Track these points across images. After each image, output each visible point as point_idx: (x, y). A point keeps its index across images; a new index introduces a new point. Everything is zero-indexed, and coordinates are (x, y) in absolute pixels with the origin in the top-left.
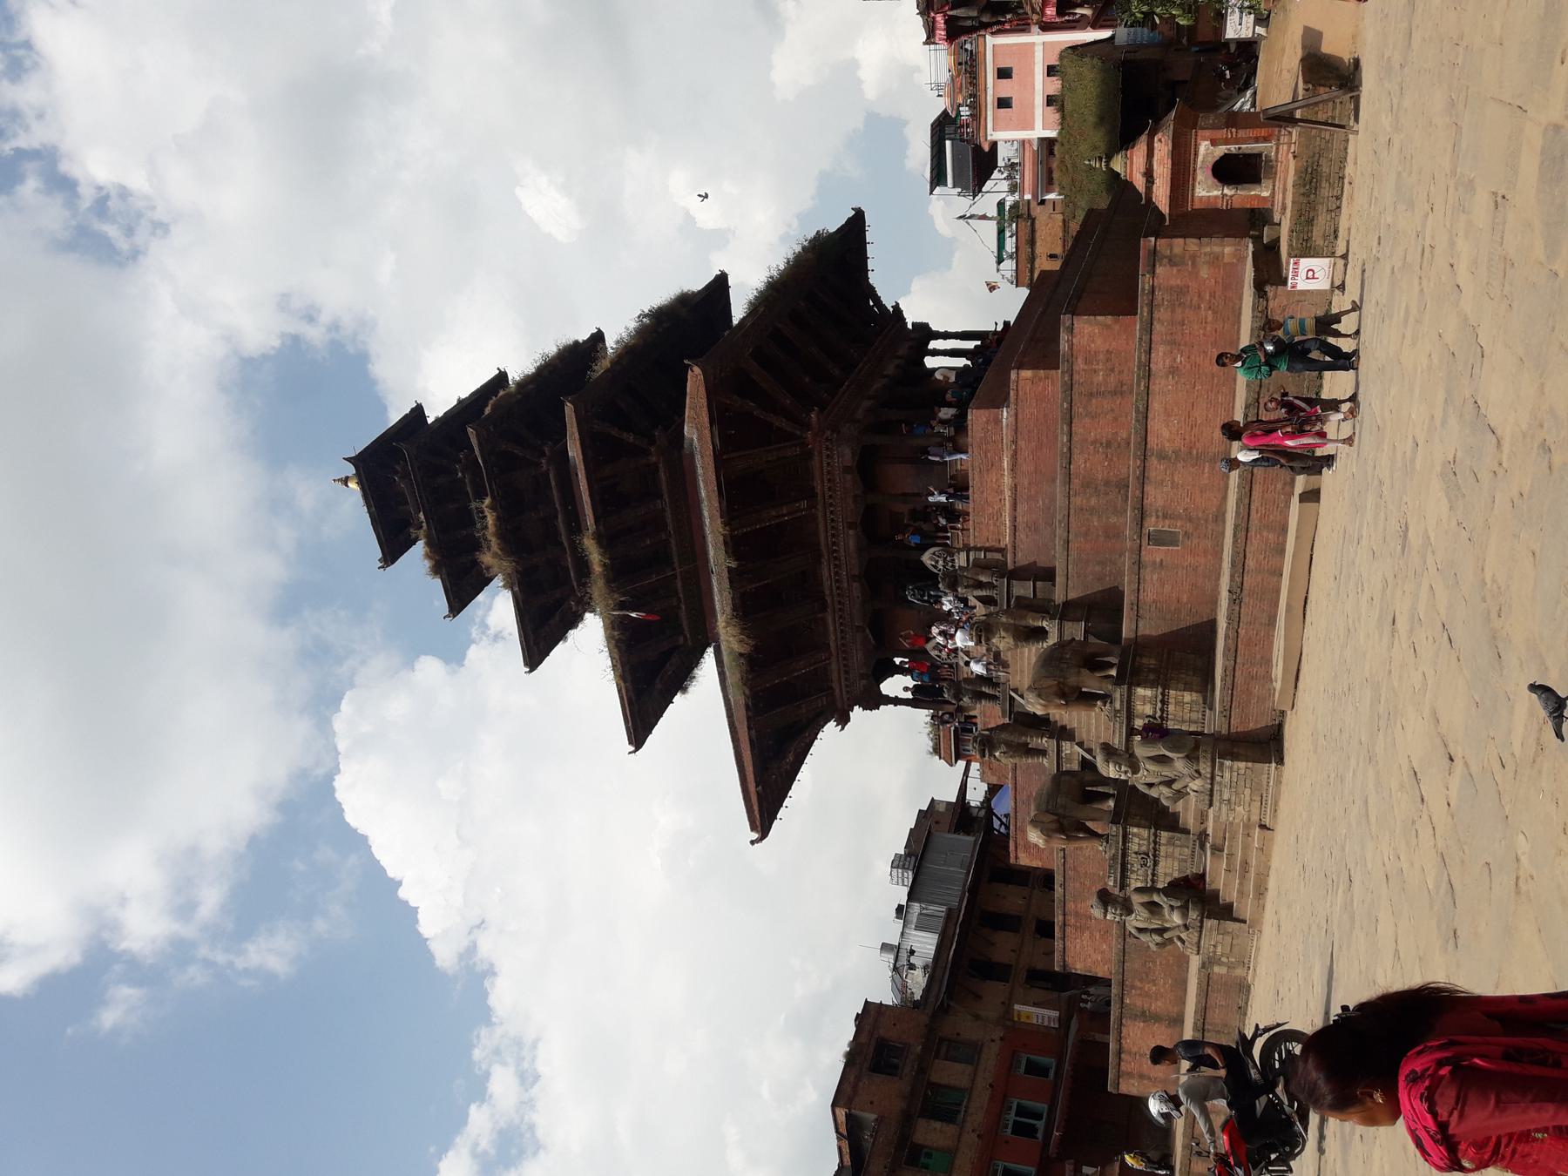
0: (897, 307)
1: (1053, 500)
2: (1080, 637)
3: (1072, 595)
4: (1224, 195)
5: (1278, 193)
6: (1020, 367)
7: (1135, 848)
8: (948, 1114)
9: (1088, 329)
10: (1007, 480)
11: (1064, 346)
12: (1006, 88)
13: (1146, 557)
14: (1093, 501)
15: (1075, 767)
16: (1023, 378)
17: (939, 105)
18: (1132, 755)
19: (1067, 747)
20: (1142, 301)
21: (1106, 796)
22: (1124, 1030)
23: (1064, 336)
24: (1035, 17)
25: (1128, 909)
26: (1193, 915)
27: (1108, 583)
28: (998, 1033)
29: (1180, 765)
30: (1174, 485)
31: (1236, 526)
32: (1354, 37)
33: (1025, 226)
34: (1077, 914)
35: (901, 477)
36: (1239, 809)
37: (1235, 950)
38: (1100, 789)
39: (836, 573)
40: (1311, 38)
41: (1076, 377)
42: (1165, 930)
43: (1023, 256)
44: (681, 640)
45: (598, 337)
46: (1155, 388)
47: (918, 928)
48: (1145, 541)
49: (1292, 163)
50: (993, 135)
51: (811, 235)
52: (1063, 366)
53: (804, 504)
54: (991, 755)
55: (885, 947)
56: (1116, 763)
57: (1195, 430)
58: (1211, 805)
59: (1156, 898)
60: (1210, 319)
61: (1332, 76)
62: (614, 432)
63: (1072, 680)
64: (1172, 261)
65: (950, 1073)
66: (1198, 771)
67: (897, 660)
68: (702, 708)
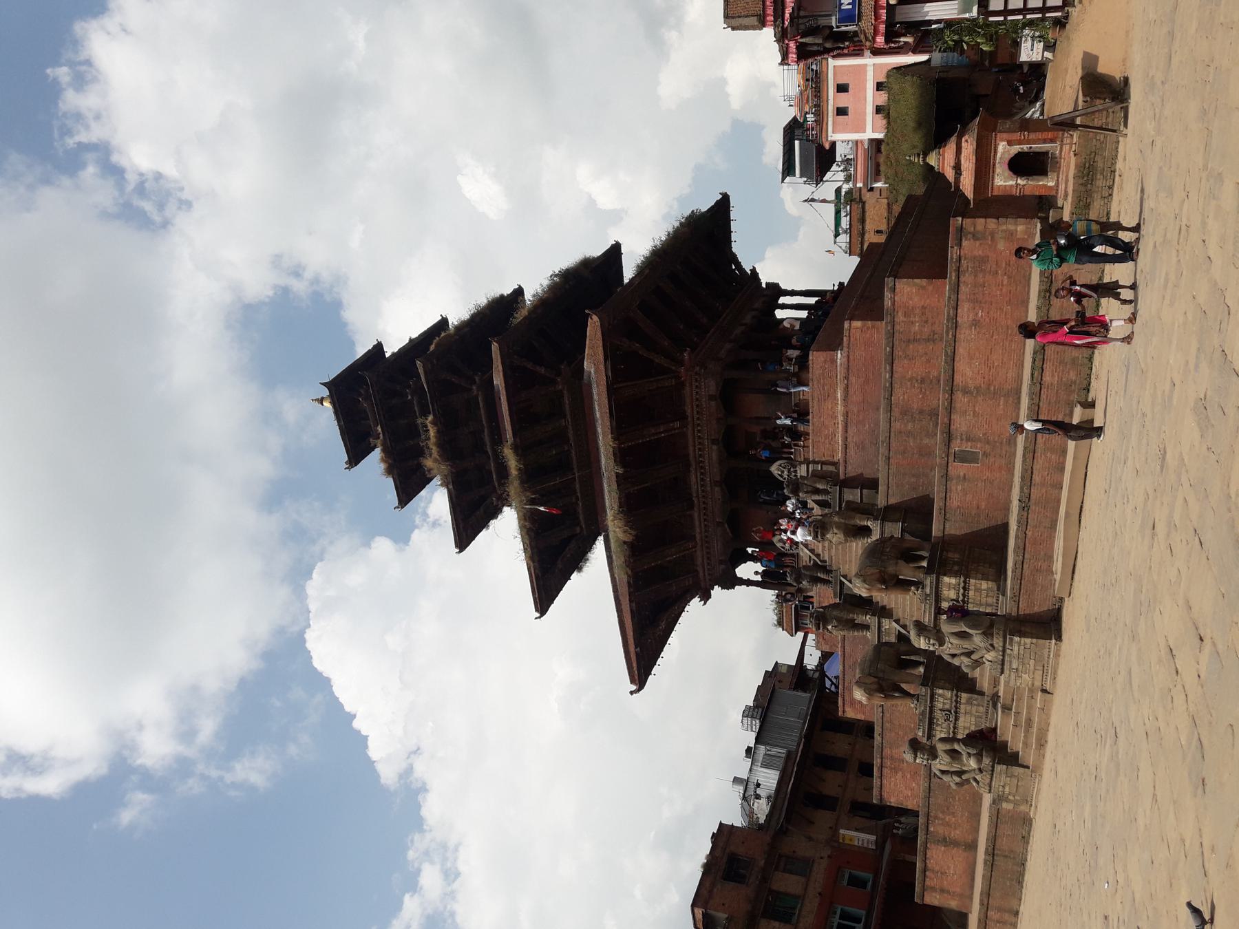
0: (754, 271)
1: (877, 424)
2: (898, 534)
3: (892, 501)
4: (1017, 185)
5: (1062, 183)
6: (851, 319)
7: (940, 706)
9: (907, 289)
10: (840, 408)
11: (887, 303)
12: (843, 100)
14: (910, 426)
15: (893, 639)
16: (854, 327)
17: (791, 113)
18: (939, 631)
19: (886, 623)
20: (951, 267)
21: (918, 664)
22: (929, 854)
23: (887, 294)
24: (868, 44)
25: (933, 754)
26: (987, 761)
28: (826, 852)
29: (978, 640)
31: (1025, 448)
32: (1124, 60)
33: (857, 207)
35: (756, 405)
36: (1025, 676)
37: (1021, 790)
38: (912, 658)
39: (702, 480)
40: (1090, 61)
41: (897, 327)
42: (964, 772)
43: (855, 232)
44: (578, 529)
45: (519, 292)
46: (960, 336)
47: (764, 765)
48: (951, 458)
49: (1073, 160)
50: (832, 136)
51: (688, 213)
52: (887, 319)
53: (677, 424)
54: (825, 628)
55: (737, 780)
56: (926, 637)
57: (993, 370)
58: (1002, 672)
59: (956, 747)
60: (1005, 282)
61: (1106, 90)
62: (530, 365)
63: (891, 569)
64: (975, 237)
65: (787, 883)
66: (992, 645)
67: (750, 550)
68: (593, 584)
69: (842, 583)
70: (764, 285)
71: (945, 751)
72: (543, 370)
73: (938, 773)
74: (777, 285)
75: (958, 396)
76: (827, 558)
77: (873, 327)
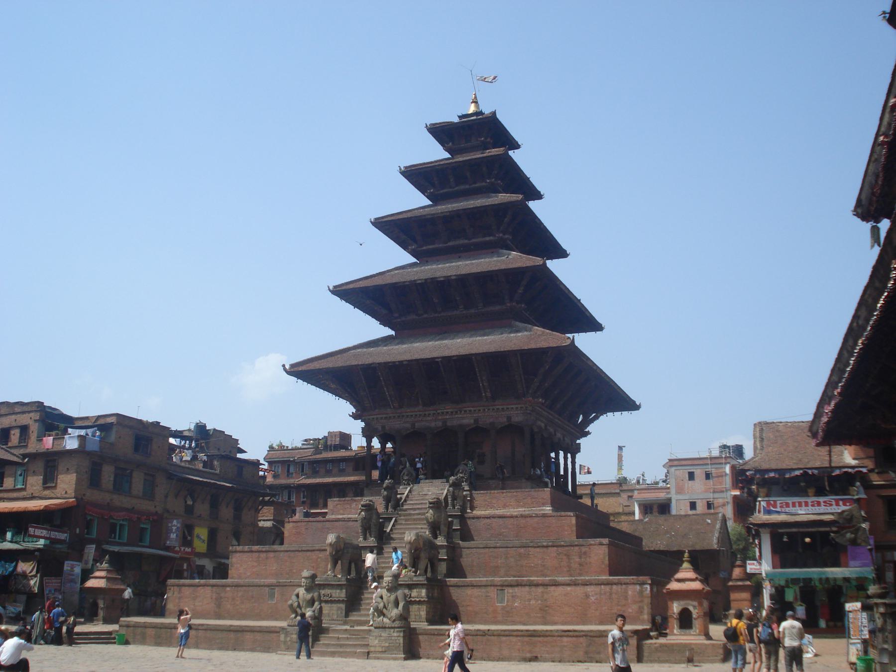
0: (588, 433)
5: (676, 636)
6: (577, 517)
8: (118, 487)
11: (591, 541)
13: (489, 589)
27: (467, 570)
28: (159, 510)
29: (395, 612)
30: (529, 600)
36: (377, 642)
53: (489, 394)
54: (362, 510)
59: (316, 603)
65: (138, 482)
66: (394, 621)
70: (578, 441)
72: (520, 291)
73: (296, 592)
75: (540, 589)
76: (405, 507)
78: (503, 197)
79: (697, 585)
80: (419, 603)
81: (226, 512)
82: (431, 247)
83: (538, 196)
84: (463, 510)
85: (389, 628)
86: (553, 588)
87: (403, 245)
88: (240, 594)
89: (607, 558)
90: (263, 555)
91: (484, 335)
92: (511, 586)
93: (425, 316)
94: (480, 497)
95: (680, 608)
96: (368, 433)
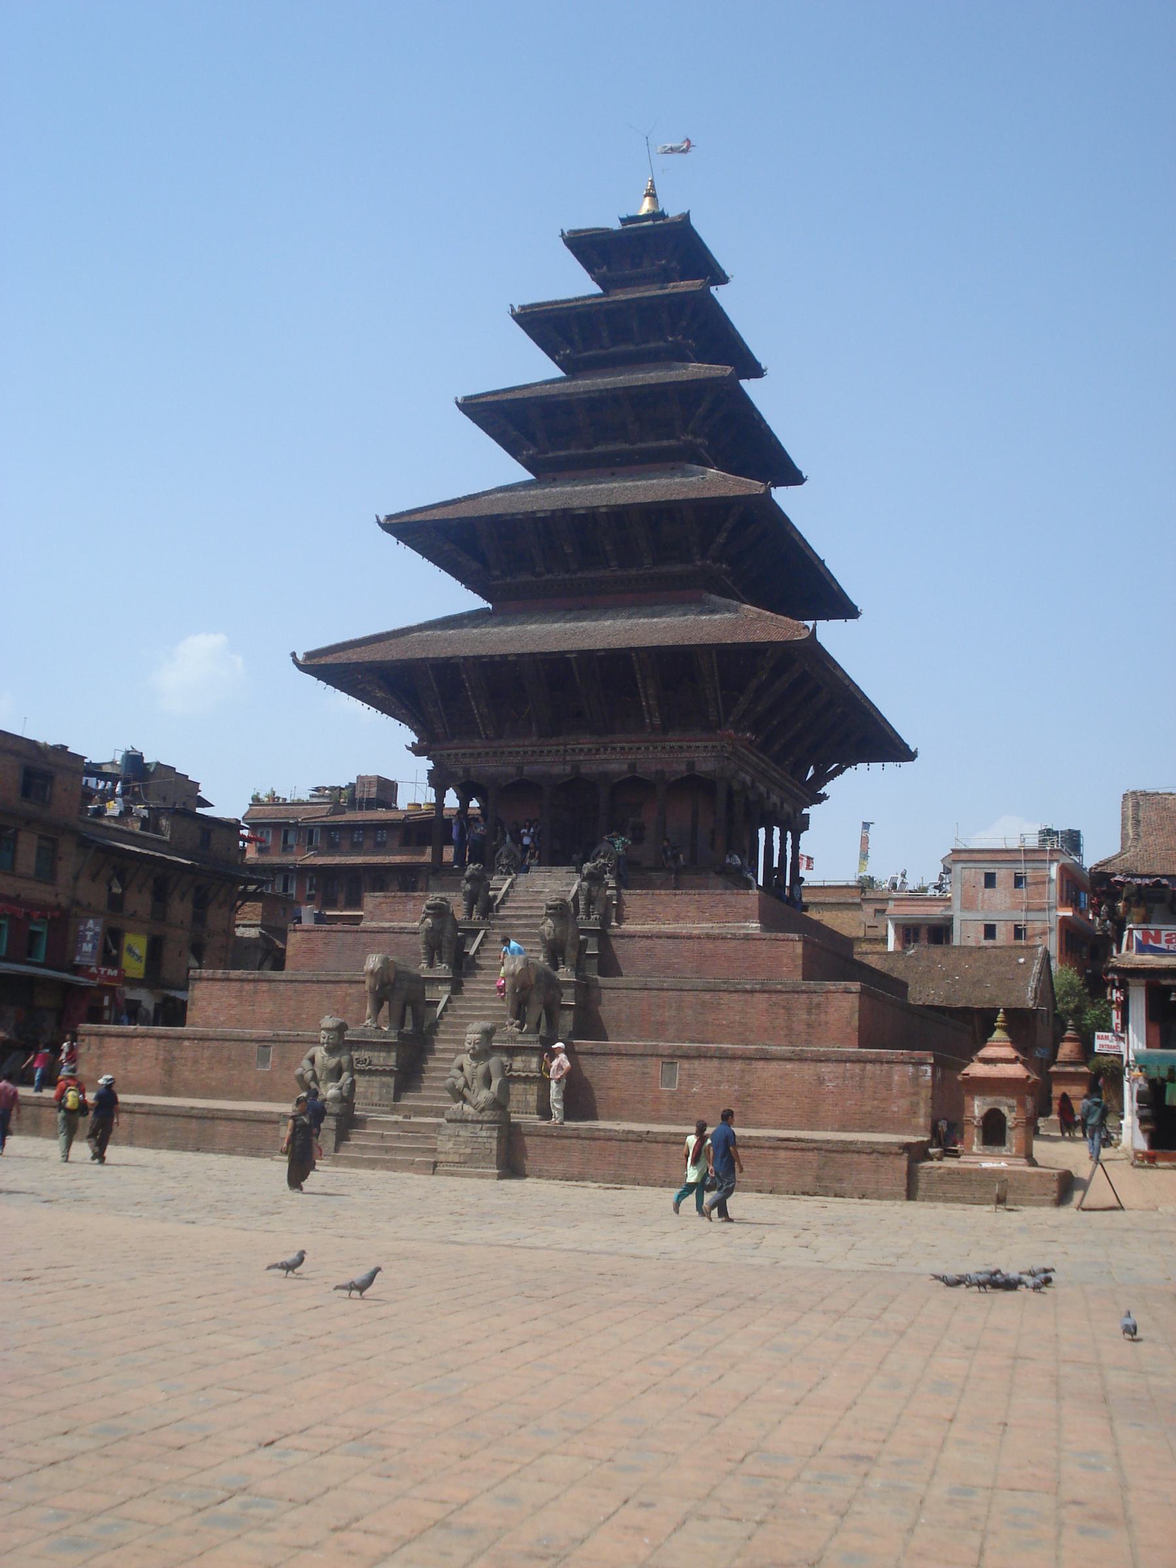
0: (824, 797)
6: (806, 942)
11: (831, 985)
28: (64, 901)
29: (484, 1095)
30: (719, 1083)
34: (256, 992)
36: (450, 1145)
39: (581, 750)
44: (497, 573)
54: (428, 915)
59: (345, 1075)
66: (483, 1110)
69: (478, 931)
70: (805, 811)
71: (339, 1063)
73: (310, 1054)
74: (807, 829)
75: (738, 1065)
77: (796, 966)
78: (696, 370)
79: (1016, 1071)
80: (526, 1080)
81: (180, 909)
82: (563, 453)
83: (757, 371)
84: (605, 921)
85: (472, 1122)
86: (760, 1064)
87: (513, 449)
88: (207, 1053)
89: (856, 1016)
90: (249, 987)
91: (654, 616)
92: (687, 1057)
93: (549, 577)
94: (634, 900)
95: (986, 1109)
96: (438, 781)
